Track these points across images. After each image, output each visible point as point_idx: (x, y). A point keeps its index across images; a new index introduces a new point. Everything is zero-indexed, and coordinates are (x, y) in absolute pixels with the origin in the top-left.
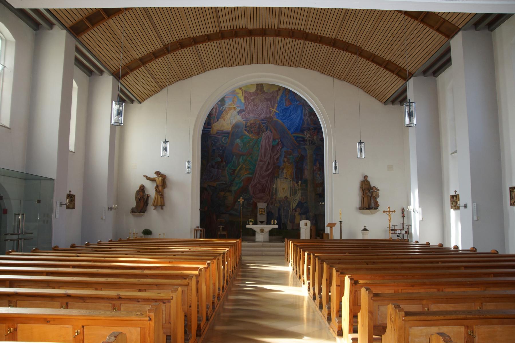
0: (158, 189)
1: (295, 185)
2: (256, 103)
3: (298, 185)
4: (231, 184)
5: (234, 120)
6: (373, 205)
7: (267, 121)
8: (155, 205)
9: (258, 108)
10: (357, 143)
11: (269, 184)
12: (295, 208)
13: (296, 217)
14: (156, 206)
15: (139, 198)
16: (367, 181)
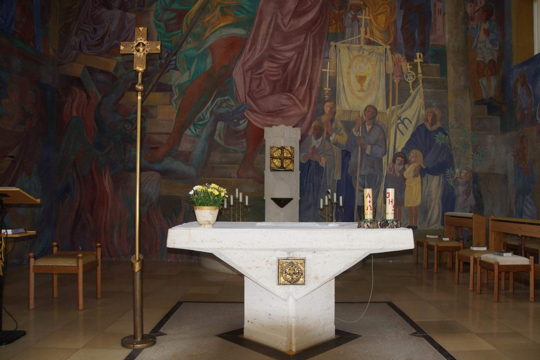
1: (401, 66)
3: (414, 68)
4: (170, 61)
11: (307, 61)
12: (403, 148)
13: (407, 181)
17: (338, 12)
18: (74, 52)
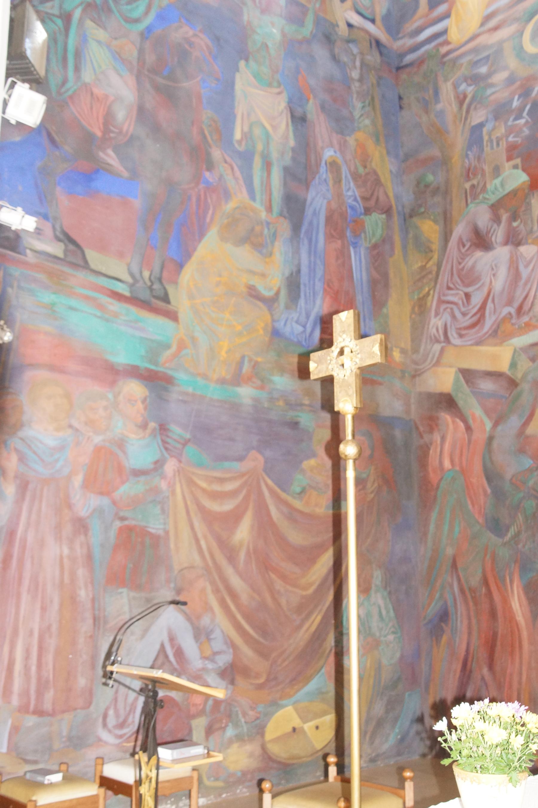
18: (437, 347)
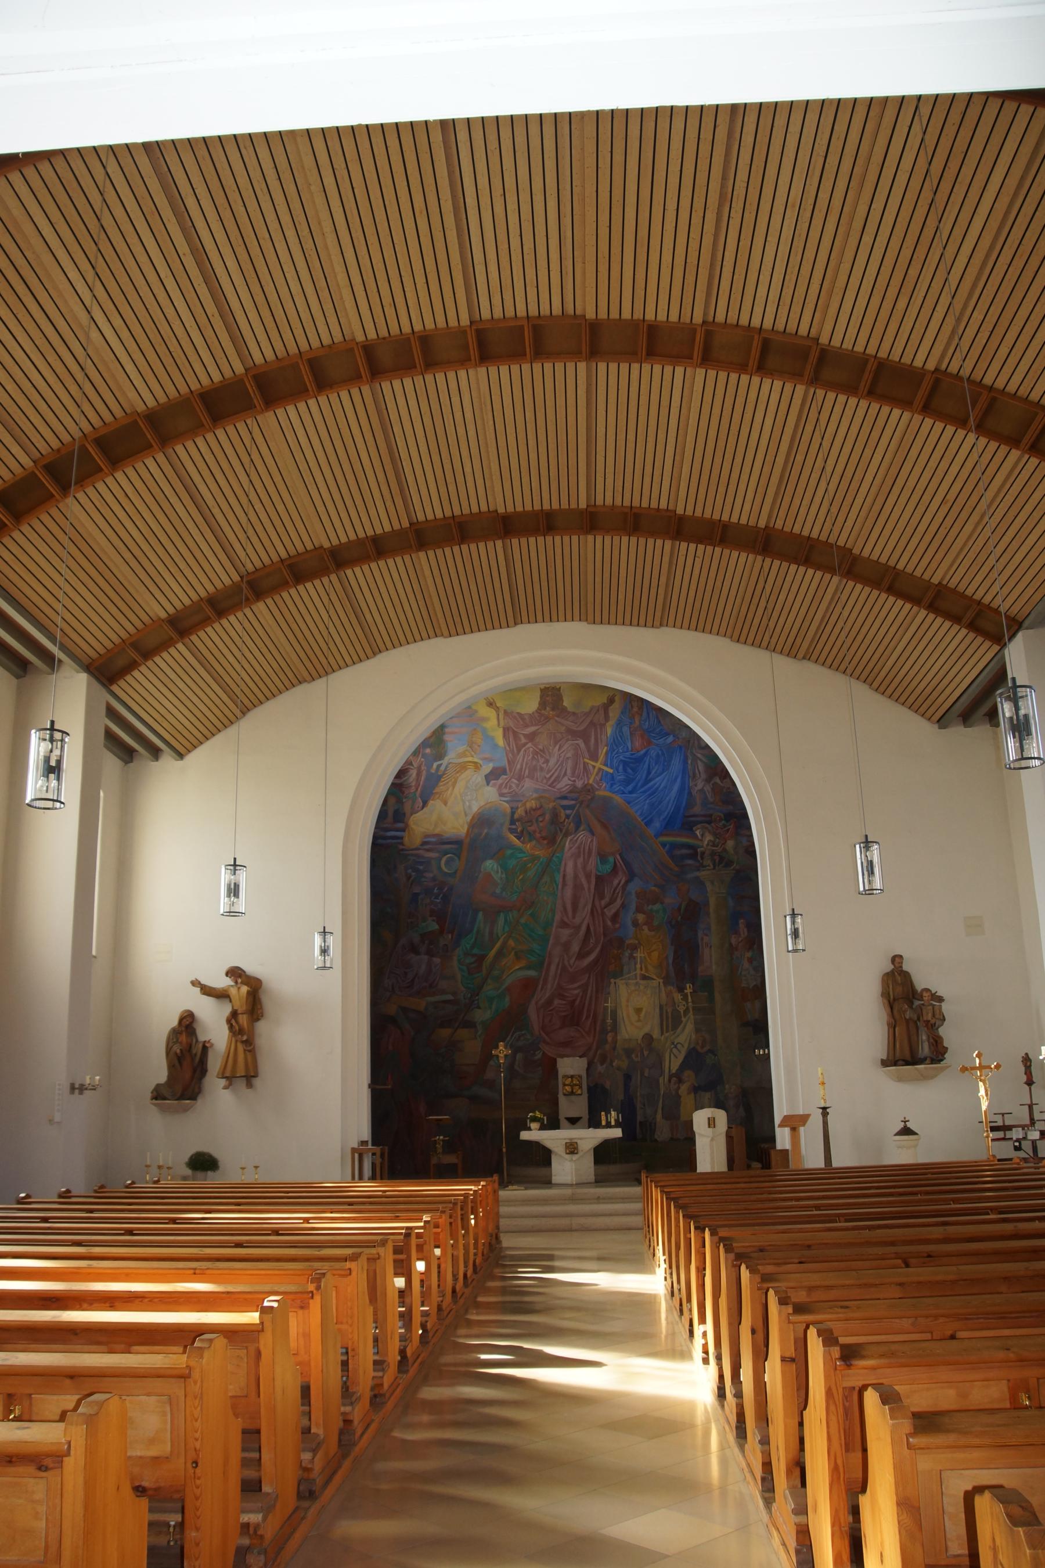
0: (237, 1022)
1: (673, 998)
2: (541, 747)
5: (474, 802)
6: (925, 1050)
7: (576, 799)
8: (228, 1074)
9: (547, 761)
10: (855, 846)
11: (591, 997)
14: (230, 1078)
15: (176, 1053)
16: (902, 971)
17: (616, 952)
